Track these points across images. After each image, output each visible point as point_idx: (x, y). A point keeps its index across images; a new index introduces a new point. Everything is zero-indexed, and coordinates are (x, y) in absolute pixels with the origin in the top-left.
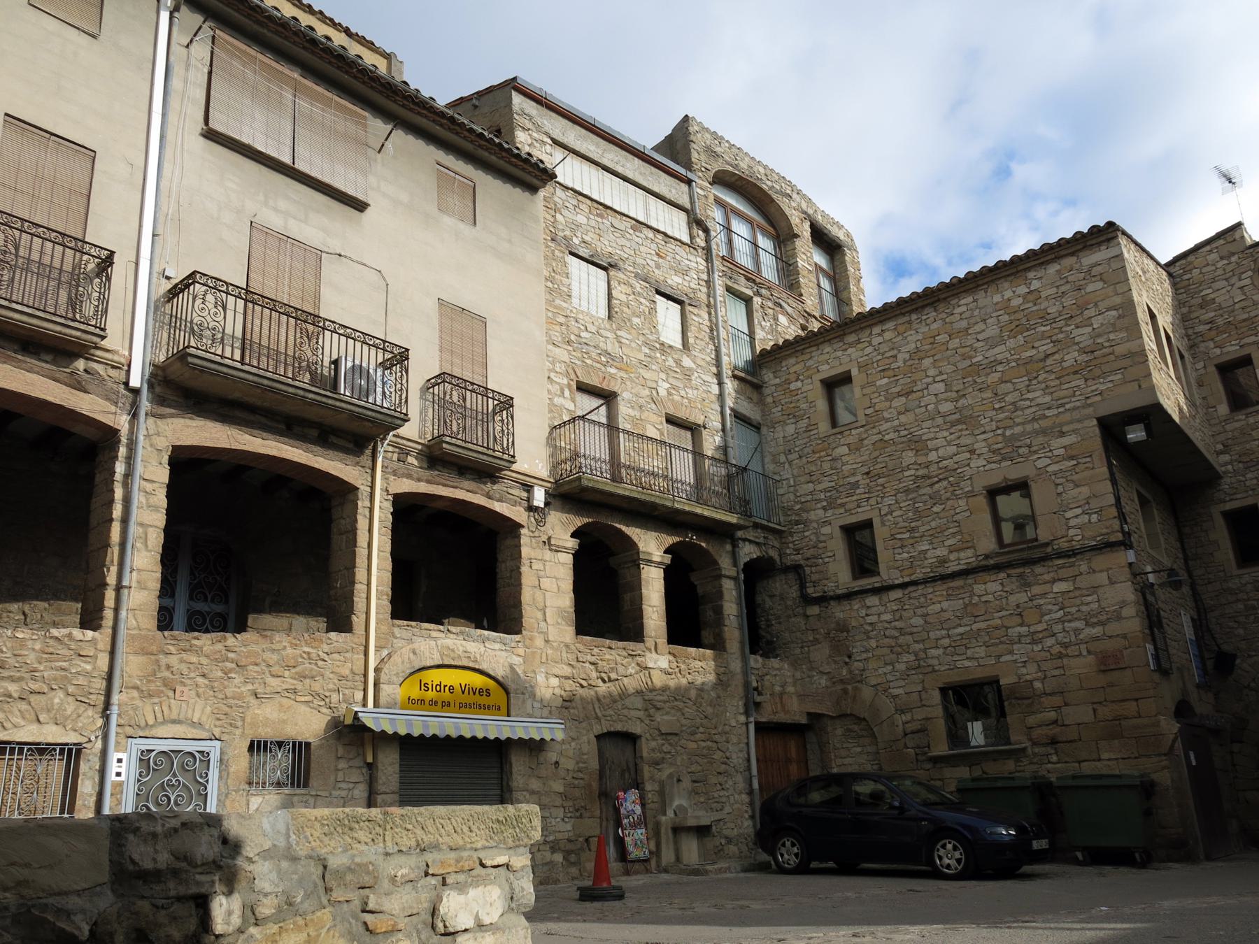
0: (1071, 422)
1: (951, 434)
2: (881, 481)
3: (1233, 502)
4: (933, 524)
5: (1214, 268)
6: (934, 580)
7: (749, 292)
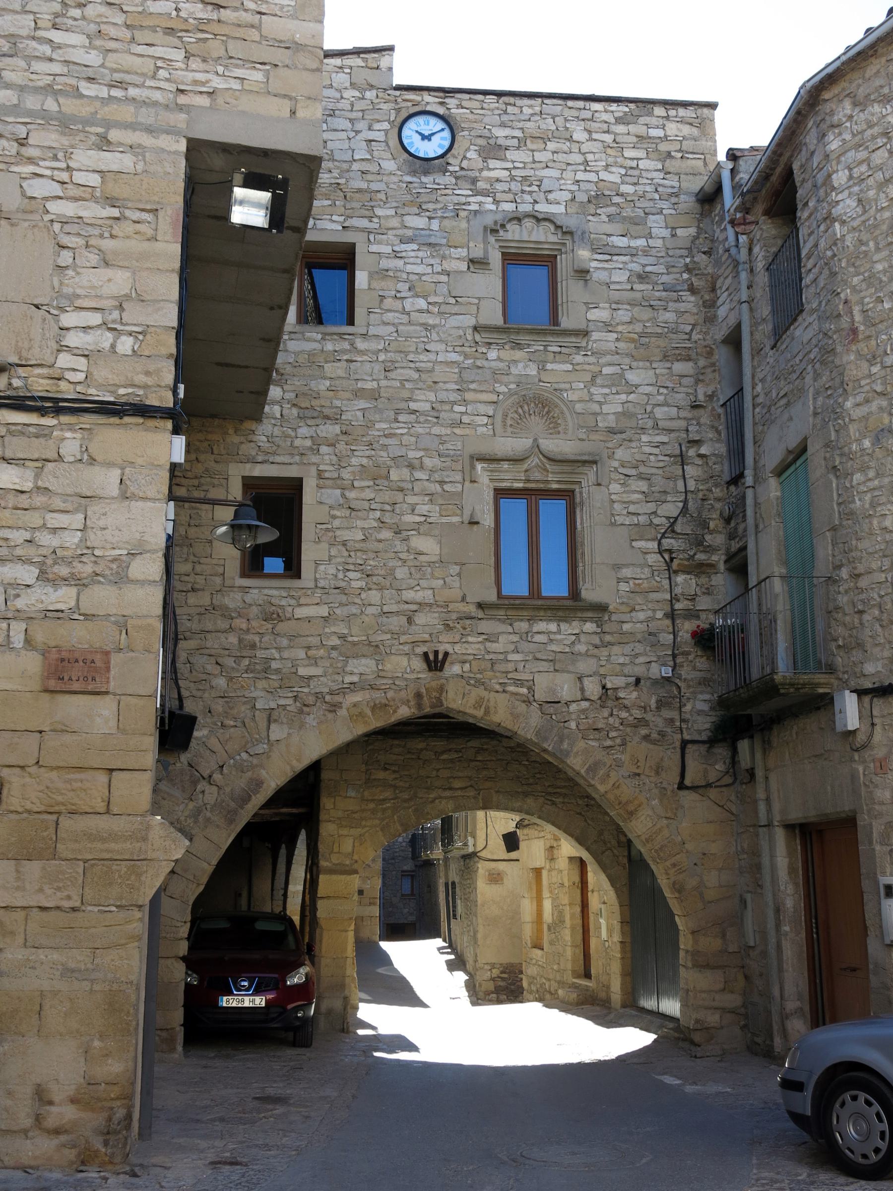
0: (132, 126)
3: (265, 466)
5: (338, 95)
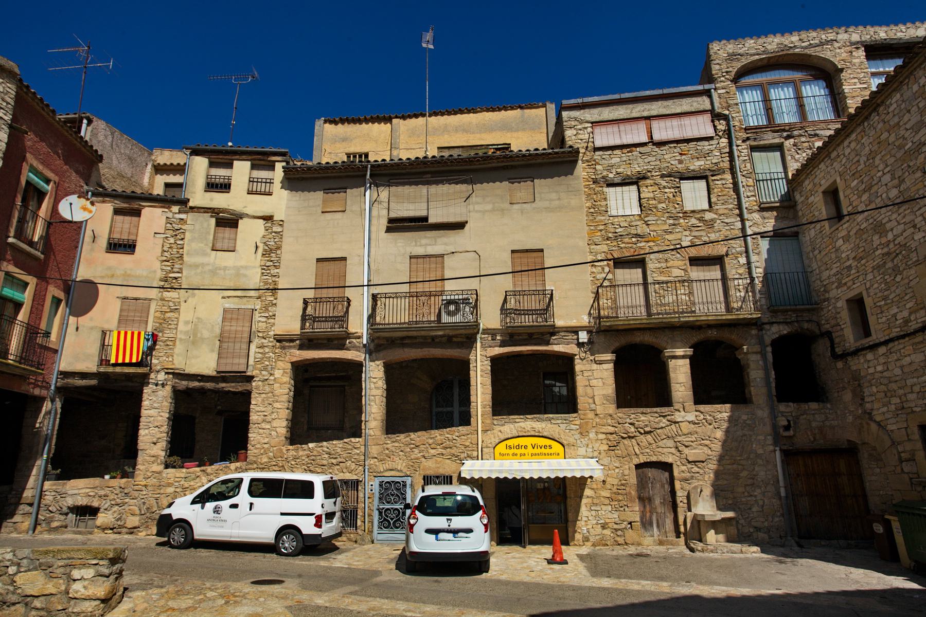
1: (899, 215)
2: (863, 262)
4: (898, 292)
6: (903, 337)
7: (777, 141)
